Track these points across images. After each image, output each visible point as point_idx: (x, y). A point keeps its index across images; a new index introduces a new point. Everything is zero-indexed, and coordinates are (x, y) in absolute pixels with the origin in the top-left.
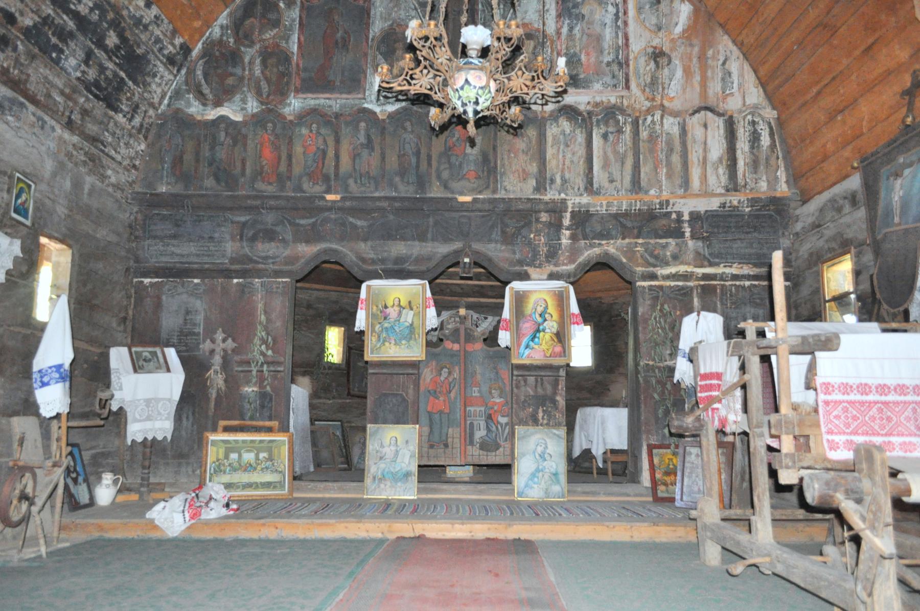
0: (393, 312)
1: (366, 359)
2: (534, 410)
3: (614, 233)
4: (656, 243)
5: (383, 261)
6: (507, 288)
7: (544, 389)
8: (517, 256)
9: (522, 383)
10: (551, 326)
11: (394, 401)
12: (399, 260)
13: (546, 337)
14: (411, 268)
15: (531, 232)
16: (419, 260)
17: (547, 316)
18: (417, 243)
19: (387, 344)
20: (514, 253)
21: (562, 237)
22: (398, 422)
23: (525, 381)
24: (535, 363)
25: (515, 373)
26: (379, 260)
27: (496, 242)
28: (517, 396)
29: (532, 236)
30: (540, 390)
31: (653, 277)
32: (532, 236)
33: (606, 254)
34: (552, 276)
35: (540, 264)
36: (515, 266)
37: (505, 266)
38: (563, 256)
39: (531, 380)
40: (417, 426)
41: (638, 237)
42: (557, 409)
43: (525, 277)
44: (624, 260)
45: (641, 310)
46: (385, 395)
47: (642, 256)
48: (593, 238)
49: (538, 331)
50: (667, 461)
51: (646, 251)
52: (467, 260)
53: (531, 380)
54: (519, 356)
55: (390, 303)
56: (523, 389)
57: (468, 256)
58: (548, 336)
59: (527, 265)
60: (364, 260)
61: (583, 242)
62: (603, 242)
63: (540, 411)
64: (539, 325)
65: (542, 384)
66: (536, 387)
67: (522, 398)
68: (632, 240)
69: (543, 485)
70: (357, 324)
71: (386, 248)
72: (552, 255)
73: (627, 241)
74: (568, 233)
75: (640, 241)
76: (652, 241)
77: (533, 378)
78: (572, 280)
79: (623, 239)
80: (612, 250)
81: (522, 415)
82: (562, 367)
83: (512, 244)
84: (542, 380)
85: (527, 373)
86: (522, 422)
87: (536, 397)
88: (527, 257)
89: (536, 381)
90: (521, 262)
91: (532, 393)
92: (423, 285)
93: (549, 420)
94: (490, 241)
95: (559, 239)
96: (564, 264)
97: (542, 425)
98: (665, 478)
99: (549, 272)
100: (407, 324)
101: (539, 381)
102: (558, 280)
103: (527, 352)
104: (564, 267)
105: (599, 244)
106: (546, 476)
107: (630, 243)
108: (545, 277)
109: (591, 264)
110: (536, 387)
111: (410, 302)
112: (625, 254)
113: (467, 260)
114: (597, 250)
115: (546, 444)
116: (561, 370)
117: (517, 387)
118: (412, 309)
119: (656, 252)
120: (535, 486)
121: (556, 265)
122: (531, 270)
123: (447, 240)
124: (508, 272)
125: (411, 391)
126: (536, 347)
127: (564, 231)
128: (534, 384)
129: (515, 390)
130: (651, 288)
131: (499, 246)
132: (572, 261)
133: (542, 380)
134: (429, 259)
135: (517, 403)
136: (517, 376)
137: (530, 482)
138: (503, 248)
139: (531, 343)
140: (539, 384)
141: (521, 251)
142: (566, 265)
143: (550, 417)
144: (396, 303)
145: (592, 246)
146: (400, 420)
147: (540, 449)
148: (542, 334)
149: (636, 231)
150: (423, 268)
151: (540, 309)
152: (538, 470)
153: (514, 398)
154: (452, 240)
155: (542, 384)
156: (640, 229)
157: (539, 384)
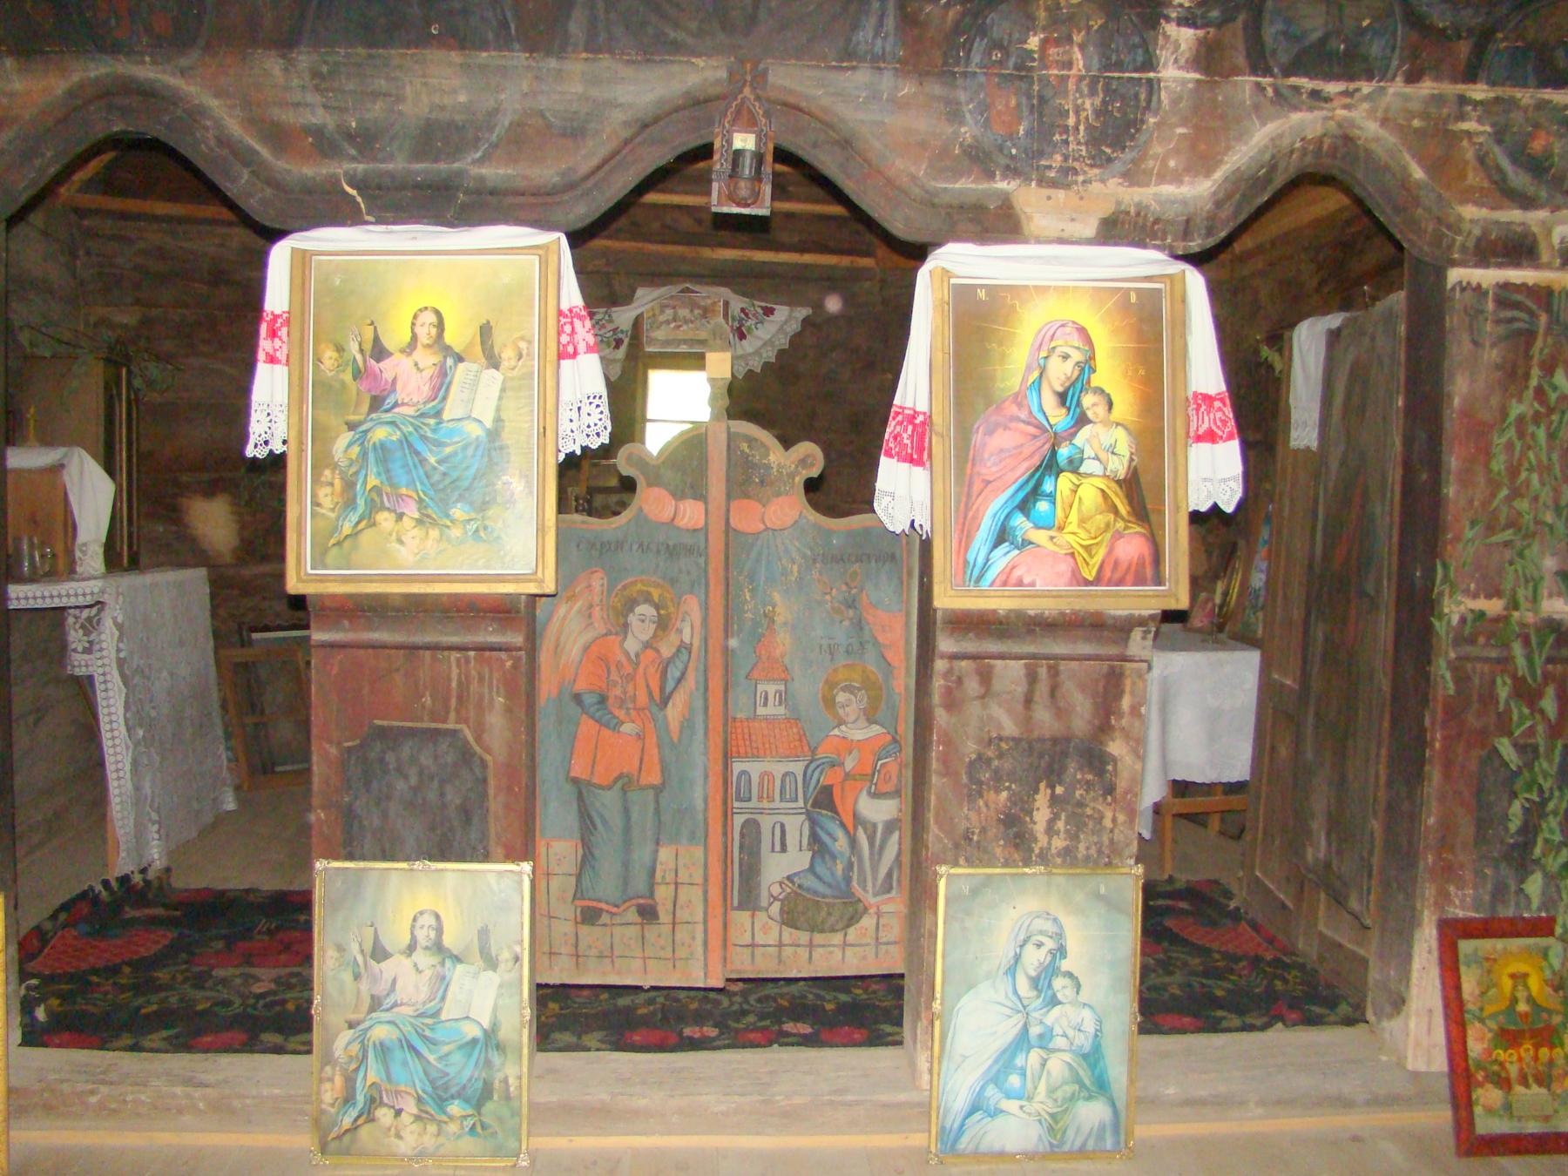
0: (409, 377)
1: (293, 585)
2: (1014, 800)
3: (1375, 49)
4: (1541, 105)
5: (365, 141)
6: (924, 275)
7: (1060, 713)
8: (968, 131)
9: (973, 686)
10: (1107, 446)
11: (426, 759)
12: (437, 137)
13: (1083, 497)
14: (495, 172)
15: (1030, 25)
16: (523, 138)
17: (1088, 400)
18: (519, 58)
19: (385, 519)
20: (955, 116)
21: (1164, 55)
22: (444, 850)
23: (986, 677)
24: (1032, 606)
25: (945, 644)
26: (350, 137)
27: (878, 62)
28: (948, 742)
29: (1034, 42)
30: (1043, 715)
31: (1519, 249)
32: (1034, 42)
33: (1346, 140)
34: (1115, 230)
35: (1066, 171)
36: (957, 174)
37: (909, 169)
38: (1164, 137)
39: (1010, 674)
40: (526, 867)
41: (1470, 77)
42: (1110, 790)
43: (997, 224)
44: (1418, 173)
45: (1461, 388)
46: (383, 733)
47: (1481, 160)
48: (1287, 73)
49: (1050, 466)
50: (1507, 983)
51: (1499, 136)
52: (744, 141)
53: (1010, 674)
54: (968, 574)
55: (396, 334)
56: (974, 710)
57: (751, 124)
58: (1089, 493)
59: (1011, 171)
60: (279, 137)
61: (1247, 81)
62: (1332, 88)
63: (1042, 799)
64: (1056, 441)
65: (1054, 690)
66: (1028, 701)
67: (970, 749)
68: (1451, 89)
69: (1042, 1102)
70: (258, 427)
71: (381, 84)
72: (1117, 133)
73: (1427, 87)
74: (1186, 37)
75: (1479, 92)
76: (1525, 96)
77: (1016, 668)
78: (1195, 245)
79: (1413, 78)
80: (1369, 128)
81: (968, 817)
82: (1142, 622)
83: (947, 75)
84: (1054, 672)
85: (992, 646)
86: (967, 848)
87: (1026, 744)
88: (1012, 136)
89: (1032, 677)
90: (980, 159)
91: (1010, 728)
92: (542, 251)
93: (1074, 837)
94: (849, 56)
95: (1150, 64)
96: (1163, 178)
97: (1044, 858)
98: (1500, 1054)
99: (1107, 209)
100: (474, 431)
101: (1044, 679)
102: (1141, 244)
103: (1002, 558)
104: (1168, 189)
105: (1315, 94)
106: (1057, 1066)
107: (1438, 99)
108: (1090, 229)
109: (1279, 180)
110: (1028, 701)
111: (486, 331)
112: (1417, 140)
113: (744, 141)
114: (1305, 123)
115: (1059, 935)
116: (1137, 634)
117: (952, 704)
118: (493, 362)
119: (1537, 146)
120: (1012, 1106)
121: (1132, 177)
122: (1029, 199)
123: (656, 47)
124: (929, 202)
125: (496, 721)
126: (1040, 537)
127: (1171, 29)
128: (1021, 689)
129: (941, 716)
130: (1506, 295)
131: (887, 81)
132: (1202, 162)
133: (1054, 672)
134: (575, 132)
135: (948, 771)
136: (954, 657)
137: (991, 1091)
138: (907, 89)
139: (1019, 520)
140: (1042, 688)
141: (984, 108)
142: (1177, 179)
143: (1078, 824)
144: (426, 333)
145: (1284, 100)
146: (449, 841)
147: (1034, 958)
148: (1065, 481)
149: (1464, 49)
150: (546, 173)
151: (1060, 372)
152: (1022, 1041)
153: (936, 751)
154: (677, 47)
155: (1054, 690)
156: (1484, 39)
157: (1042, 688)
